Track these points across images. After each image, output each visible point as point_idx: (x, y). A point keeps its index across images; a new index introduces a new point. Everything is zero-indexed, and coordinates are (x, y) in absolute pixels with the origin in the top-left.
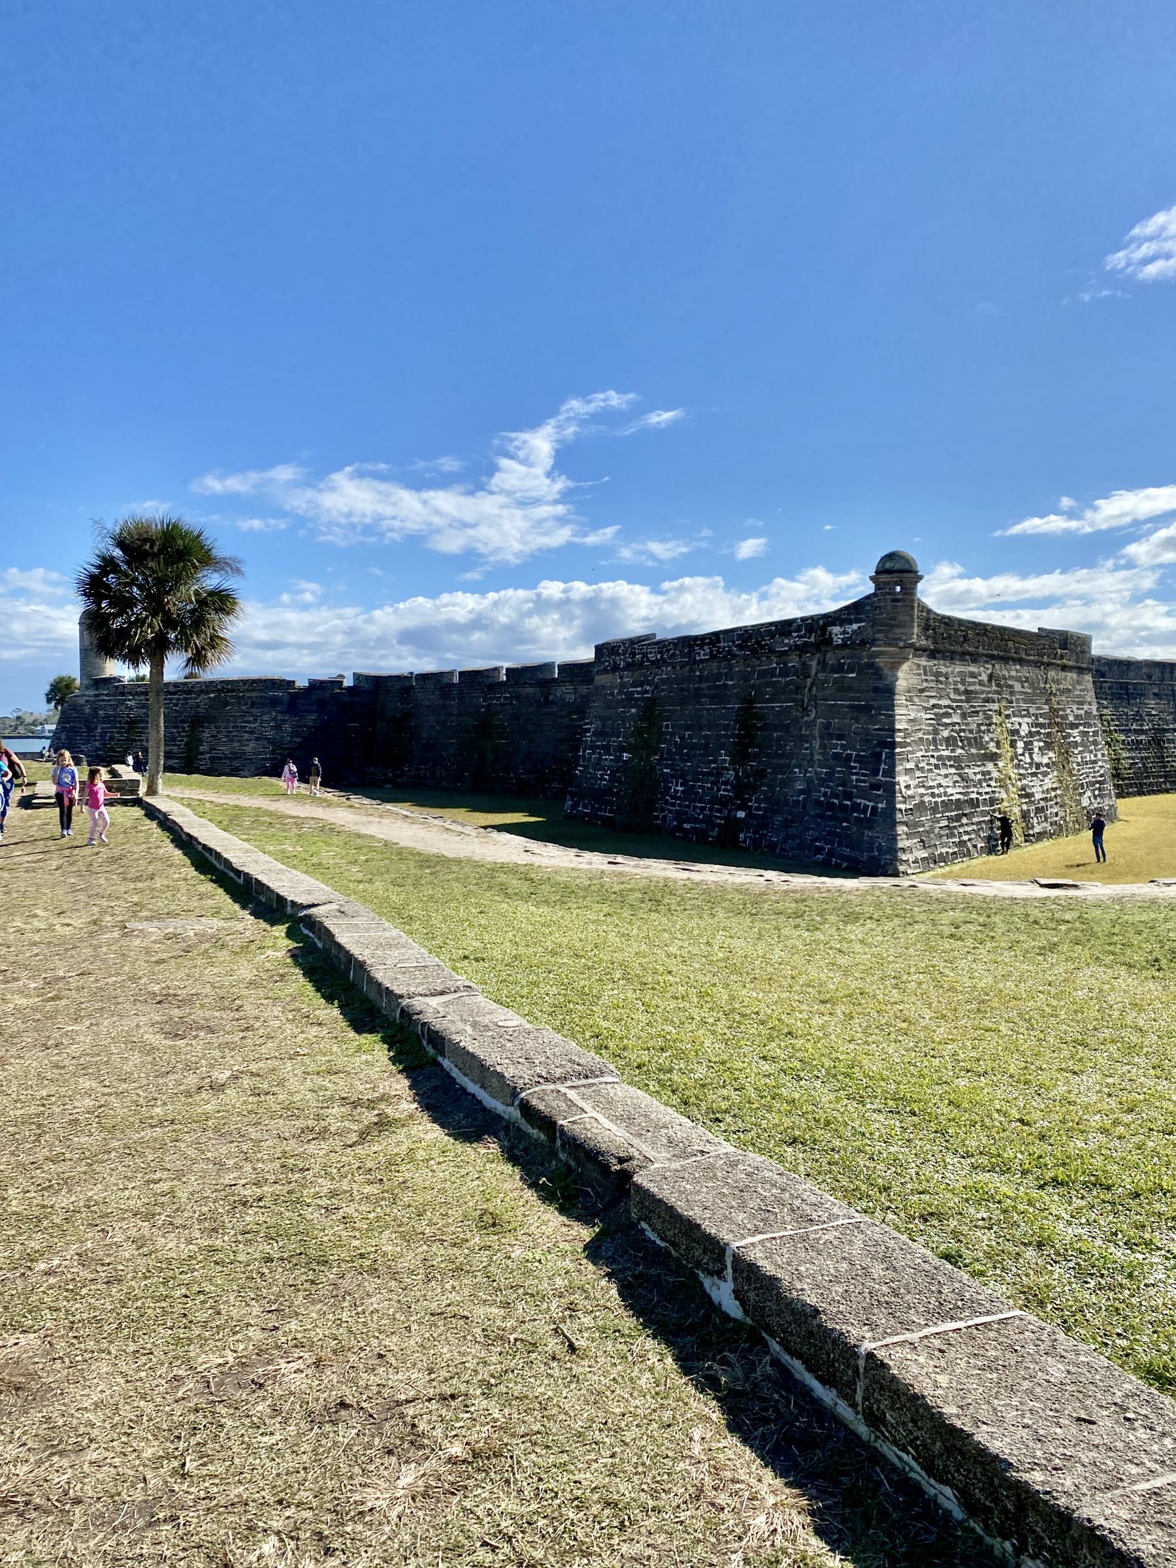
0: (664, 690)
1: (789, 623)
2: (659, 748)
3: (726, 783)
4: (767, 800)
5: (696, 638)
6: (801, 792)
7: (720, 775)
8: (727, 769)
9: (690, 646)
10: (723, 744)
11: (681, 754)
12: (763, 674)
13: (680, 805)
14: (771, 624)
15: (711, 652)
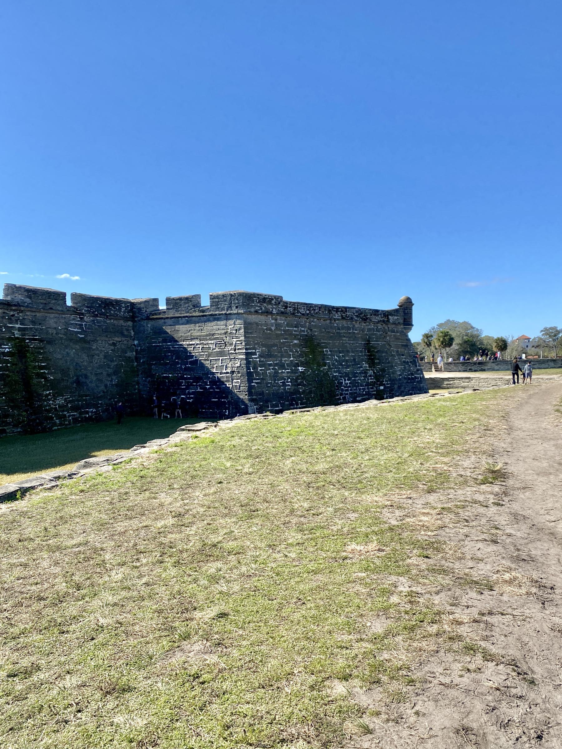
0: (315, 331)
1: (377, 311)
2: (326, 363)
3: (371, 376)
4: (390, 380)
5: (333, 307)
6: (400, 375)
7: (366, 373)
8: (367, 370)
9: (329, 311)
10: (362, 359)
11: (342, 365)
12: (369, 330)
13: (351, 390)
14: (370, 310)
15: (342, 316)
